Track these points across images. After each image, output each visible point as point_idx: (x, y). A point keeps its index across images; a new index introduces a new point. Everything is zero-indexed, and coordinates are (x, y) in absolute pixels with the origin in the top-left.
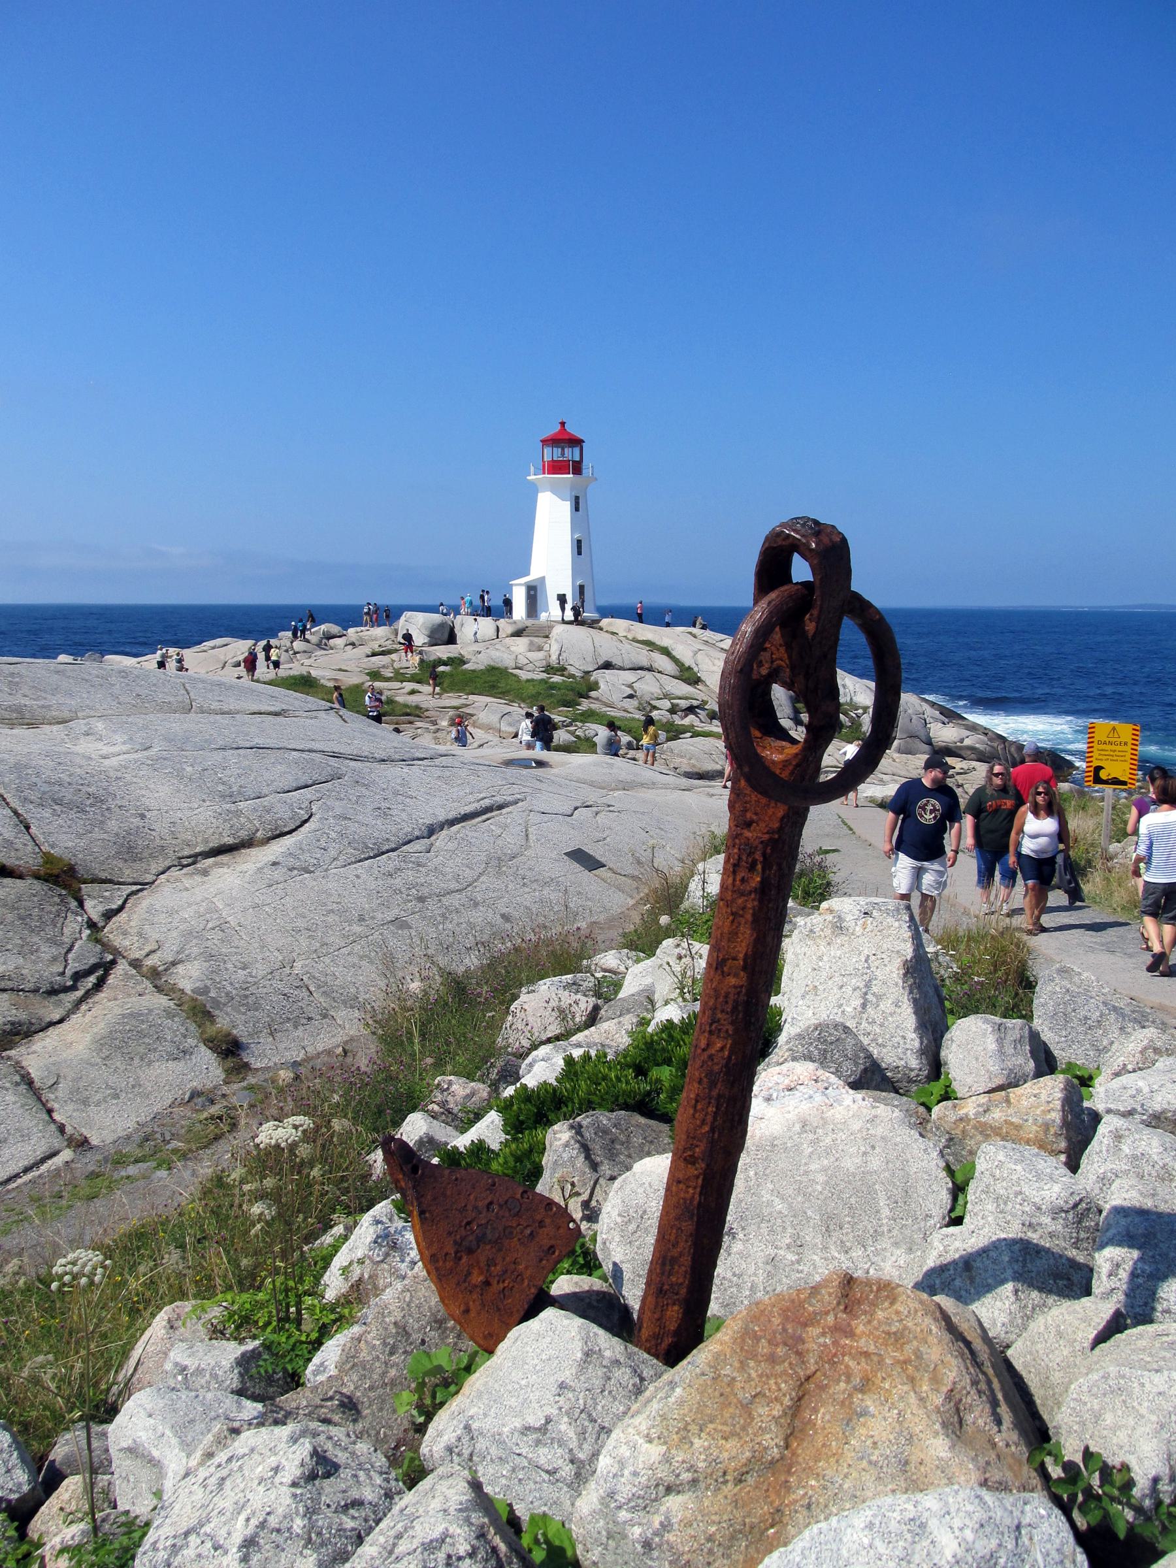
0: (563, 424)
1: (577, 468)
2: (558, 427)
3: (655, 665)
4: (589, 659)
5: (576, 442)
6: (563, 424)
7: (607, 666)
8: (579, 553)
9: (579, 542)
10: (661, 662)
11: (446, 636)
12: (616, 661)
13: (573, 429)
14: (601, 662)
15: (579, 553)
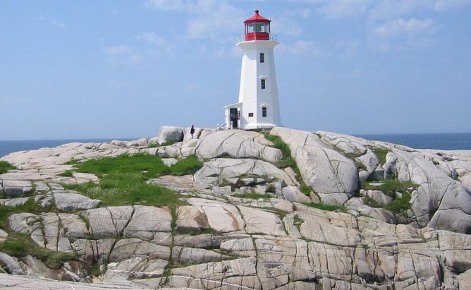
0: (257, 12)
1: (265, 36)
2: (255, 14)
3: (262, 155)
4: (213, 152)
5: (267, 22)
6: (257, 12)
7: (226, 155)
8: (263, 87)
9: (263, 81)
10: (272, 153)
11: (177, 138)
12: (233, 153)
13: (263, 15)
14: (220, 153)
15: (263, 87)
